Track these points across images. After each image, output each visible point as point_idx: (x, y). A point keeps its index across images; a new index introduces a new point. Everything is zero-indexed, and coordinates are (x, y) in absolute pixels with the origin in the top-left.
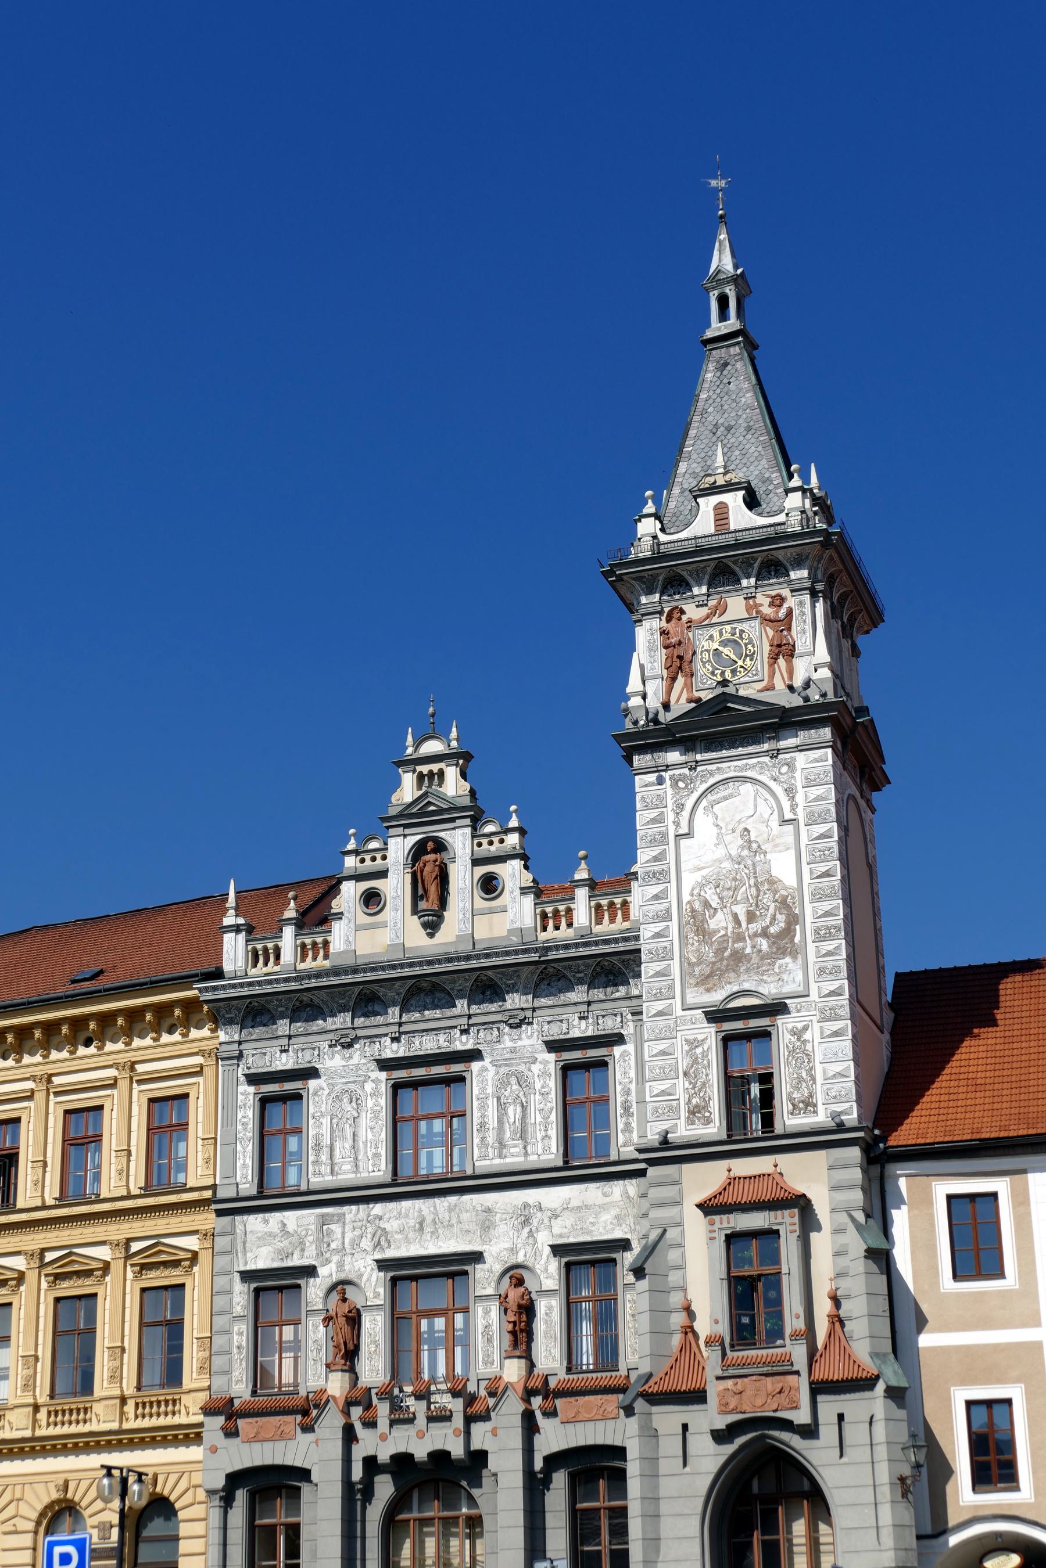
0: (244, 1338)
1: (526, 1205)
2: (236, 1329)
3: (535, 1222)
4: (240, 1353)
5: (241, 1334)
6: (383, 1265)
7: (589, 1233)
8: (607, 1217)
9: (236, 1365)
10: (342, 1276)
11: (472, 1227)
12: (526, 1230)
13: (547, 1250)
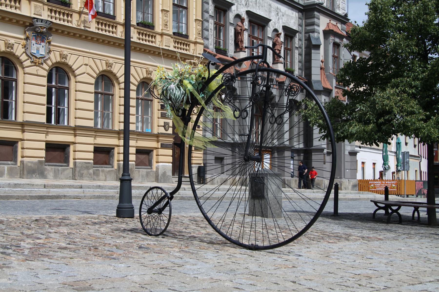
0: (212, 26)
1: (278, 8)
2: (210, 21)
3: (279, 15)
4: (211, 32)
5: (211, 23)
6: (249, 13)
7: (289, 25)
8: (292, 21)
9: (210, 37)
10: (238, 12)
11: (267, 9)
12: (278, 17)
13: (281, 27)
